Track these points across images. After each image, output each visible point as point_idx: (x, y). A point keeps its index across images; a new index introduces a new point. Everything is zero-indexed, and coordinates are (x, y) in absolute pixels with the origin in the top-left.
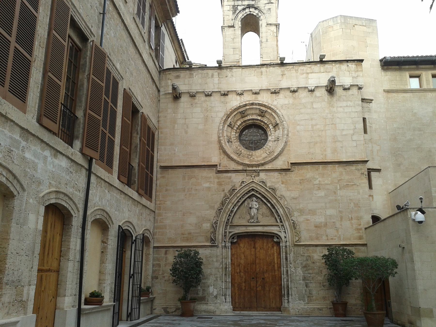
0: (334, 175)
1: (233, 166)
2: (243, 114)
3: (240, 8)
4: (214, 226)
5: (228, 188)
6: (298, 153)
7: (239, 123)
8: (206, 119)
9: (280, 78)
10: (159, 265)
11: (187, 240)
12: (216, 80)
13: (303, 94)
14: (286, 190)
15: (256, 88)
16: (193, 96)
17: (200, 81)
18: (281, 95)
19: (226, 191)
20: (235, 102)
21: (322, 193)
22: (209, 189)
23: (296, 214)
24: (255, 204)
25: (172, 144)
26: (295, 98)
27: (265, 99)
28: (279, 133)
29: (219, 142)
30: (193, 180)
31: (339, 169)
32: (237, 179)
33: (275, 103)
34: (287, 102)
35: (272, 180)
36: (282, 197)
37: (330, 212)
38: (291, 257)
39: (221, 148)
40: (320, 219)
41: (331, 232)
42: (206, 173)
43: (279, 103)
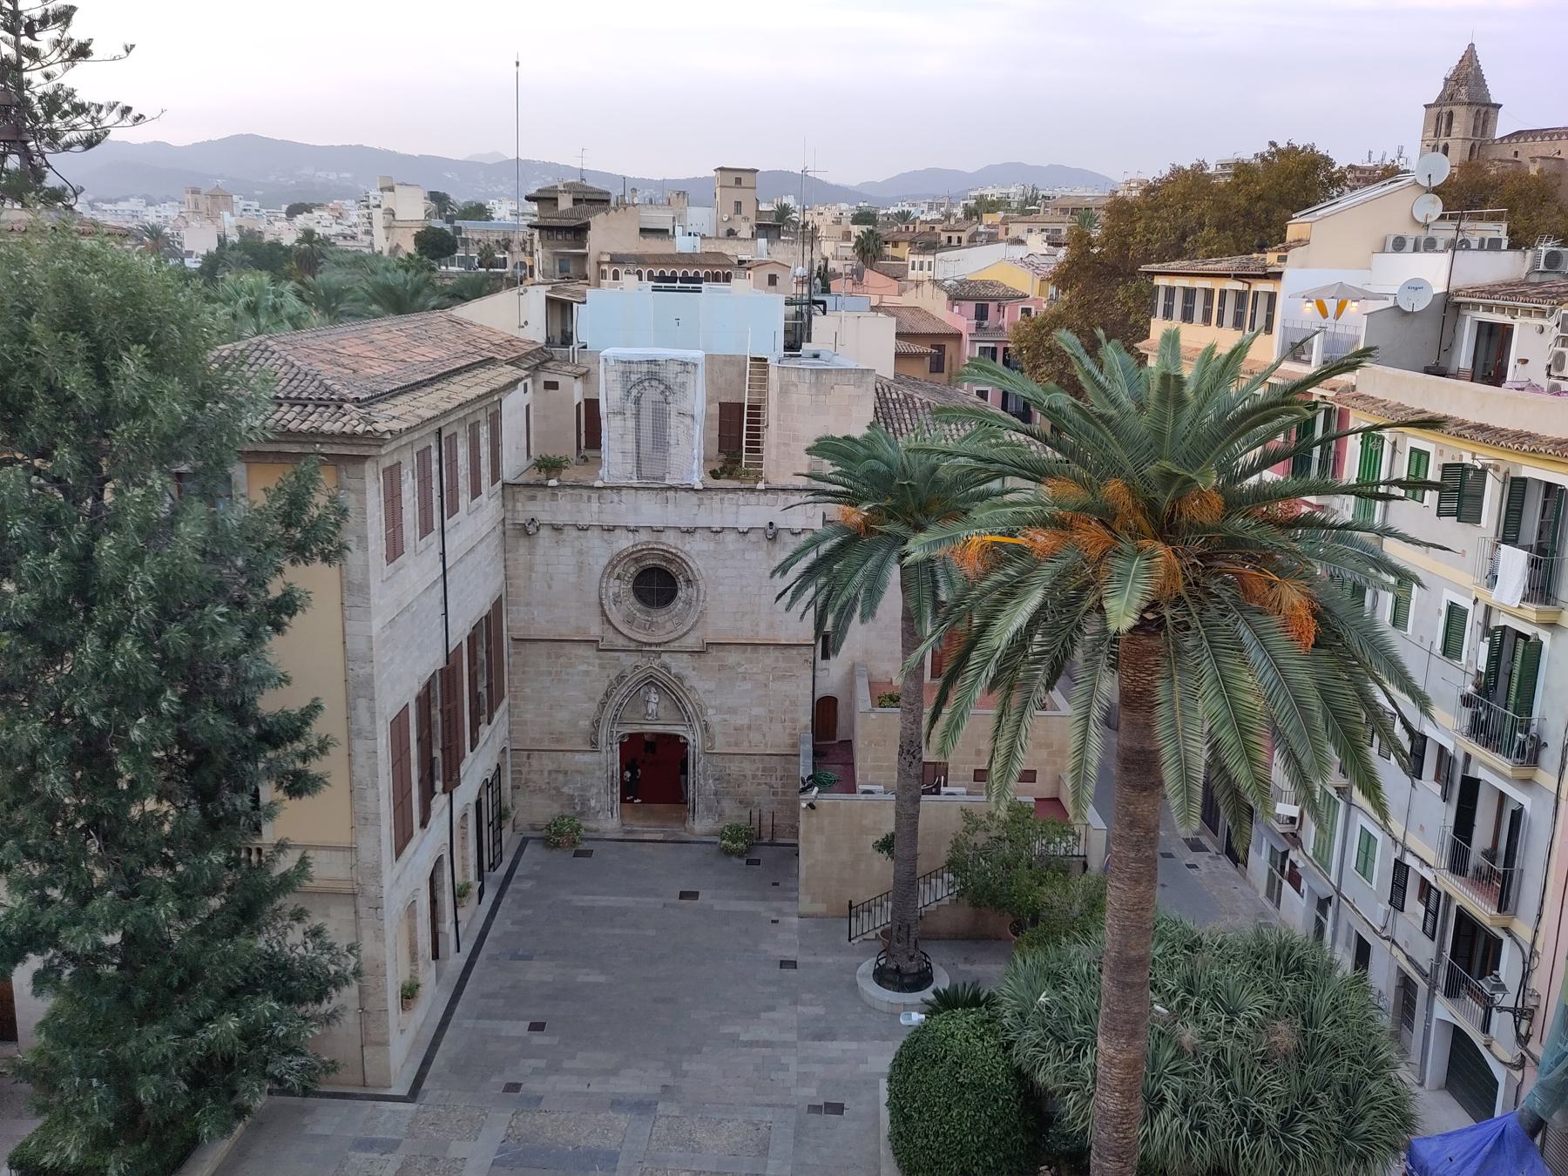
0: (767, 661)
1: (620, 642)
2: (637, 560)
3: (634, 377)
4: (596, 724)
5: (614, 674)
6: (719, 626)
7: (632, 570)
8: (581, 567)
9: (695, 510)
10: (520, 772)
11: (558, 741)
12: (595, 506)
13: (730, 537)
14: (700, 682)
15: (658, 524)
16: (557, 529)
17: (569, 507)
18: (697, 535)
19: (612, 677)
20: (624, 542)
21: (749, 686)
22: (587, 673)
23: (710, 712)
24: (654, 697)
25: (528, 604)
26: (718, 543)
27: (671, 540)
28: (692, 591)
29: (602, 605)
30: (562, 660)
31: (774, 654)
32: (628, 660)
33: (687, 548)
34: (705, 547)
35: (679, 664)
36: (692, 688)
37: (756, 711)
38: (700, 768)
39: (604, 613)
40: (741, 720)
41: (755, 737)
42: (581, 650)
43: (696, 552)
